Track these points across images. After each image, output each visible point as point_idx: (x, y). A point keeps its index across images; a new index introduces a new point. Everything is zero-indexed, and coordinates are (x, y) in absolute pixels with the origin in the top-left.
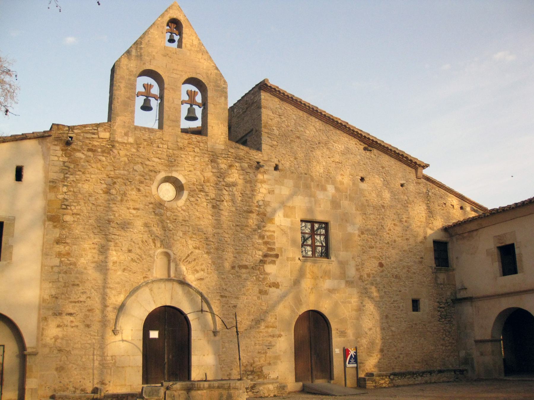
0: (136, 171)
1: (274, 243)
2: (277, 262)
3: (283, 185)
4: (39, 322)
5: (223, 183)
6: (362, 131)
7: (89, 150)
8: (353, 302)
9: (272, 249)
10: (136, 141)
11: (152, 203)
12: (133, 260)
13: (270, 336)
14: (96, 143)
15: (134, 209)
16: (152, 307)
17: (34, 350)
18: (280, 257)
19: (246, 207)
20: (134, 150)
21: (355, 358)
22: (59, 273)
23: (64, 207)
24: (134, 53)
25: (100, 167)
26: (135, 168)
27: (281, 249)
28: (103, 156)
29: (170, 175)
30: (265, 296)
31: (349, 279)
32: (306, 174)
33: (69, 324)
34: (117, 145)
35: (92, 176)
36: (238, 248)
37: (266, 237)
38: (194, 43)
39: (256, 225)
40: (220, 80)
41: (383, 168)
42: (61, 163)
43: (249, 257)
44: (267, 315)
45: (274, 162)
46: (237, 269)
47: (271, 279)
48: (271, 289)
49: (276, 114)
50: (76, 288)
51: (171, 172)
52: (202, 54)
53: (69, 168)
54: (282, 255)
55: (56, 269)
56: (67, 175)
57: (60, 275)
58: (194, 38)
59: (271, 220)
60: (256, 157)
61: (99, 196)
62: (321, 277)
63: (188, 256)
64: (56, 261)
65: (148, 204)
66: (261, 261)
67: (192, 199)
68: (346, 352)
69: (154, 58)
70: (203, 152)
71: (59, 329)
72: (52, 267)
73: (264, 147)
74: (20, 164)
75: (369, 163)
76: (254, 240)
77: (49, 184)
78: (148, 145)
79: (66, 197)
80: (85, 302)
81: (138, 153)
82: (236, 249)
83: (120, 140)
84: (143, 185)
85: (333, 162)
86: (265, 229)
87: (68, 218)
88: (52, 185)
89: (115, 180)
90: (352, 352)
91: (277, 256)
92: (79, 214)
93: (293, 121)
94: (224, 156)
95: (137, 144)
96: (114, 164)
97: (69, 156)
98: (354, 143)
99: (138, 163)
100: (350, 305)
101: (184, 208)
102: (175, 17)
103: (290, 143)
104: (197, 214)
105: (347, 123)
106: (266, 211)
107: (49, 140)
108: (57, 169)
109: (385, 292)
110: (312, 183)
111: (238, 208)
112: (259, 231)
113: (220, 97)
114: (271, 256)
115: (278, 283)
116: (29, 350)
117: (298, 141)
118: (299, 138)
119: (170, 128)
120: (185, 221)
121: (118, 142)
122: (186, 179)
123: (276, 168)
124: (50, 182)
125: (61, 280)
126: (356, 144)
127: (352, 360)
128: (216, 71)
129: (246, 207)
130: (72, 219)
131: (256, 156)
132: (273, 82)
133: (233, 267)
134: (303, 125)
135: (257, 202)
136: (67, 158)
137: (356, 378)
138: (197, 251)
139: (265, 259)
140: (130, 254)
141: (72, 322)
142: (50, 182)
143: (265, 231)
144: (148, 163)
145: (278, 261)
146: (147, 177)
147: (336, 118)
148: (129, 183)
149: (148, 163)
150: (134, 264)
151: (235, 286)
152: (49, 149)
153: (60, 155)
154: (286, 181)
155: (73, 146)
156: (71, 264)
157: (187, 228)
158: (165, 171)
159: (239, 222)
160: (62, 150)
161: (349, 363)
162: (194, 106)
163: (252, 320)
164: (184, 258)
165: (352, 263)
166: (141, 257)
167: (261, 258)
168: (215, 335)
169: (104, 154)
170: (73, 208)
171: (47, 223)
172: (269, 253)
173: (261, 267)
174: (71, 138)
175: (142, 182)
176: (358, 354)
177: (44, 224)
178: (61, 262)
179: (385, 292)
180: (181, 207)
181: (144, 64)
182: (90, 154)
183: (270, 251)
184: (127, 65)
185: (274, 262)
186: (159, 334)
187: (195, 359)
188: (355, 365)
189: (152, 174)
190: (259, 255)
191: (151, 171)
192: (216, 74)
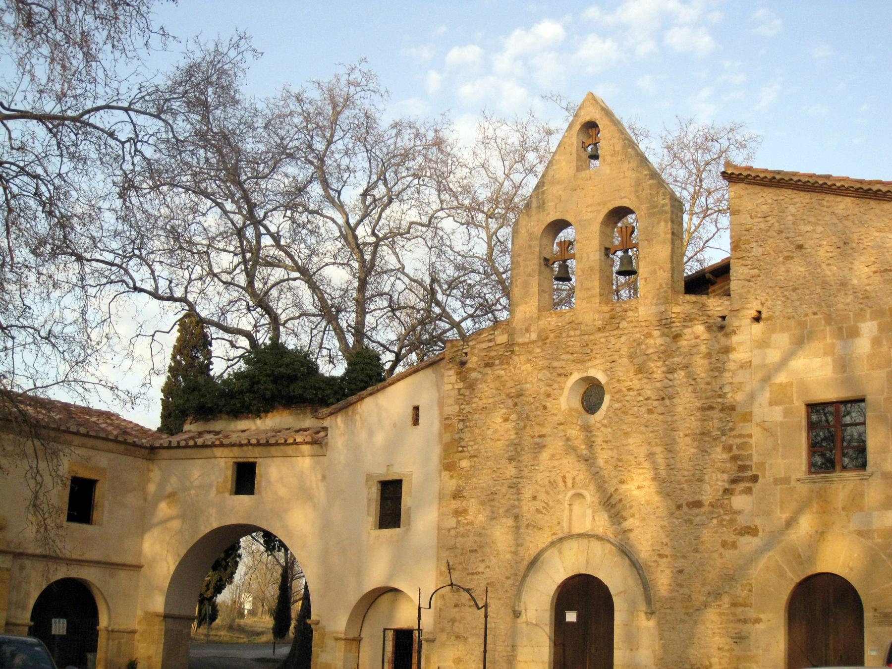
1: (750, 457)
2: (754, 490)
9: (742, 468)
10: (539, 336)
13: (740, 620)
14: (493, 354)
15: (540, 436)
17: (430, 636)
18: (760, 480)
19: (701, 402)
20: (538, 350)
23: (460, 449)
24: (534, 204)
28: (502, 369)
29: (585, 375)
30: (731, 551)
32: (815, 314)
37: (734, 447)
39: (718, 429)
42: (456, 391)
44: (734, 583)
45: (751, 308)
46: (685, 509)
47: (742, 521)
49: (756, 217)
50: (474, 554)
51: (586, 371)
52: (629, 162)
53: (465, 396)
54: (764, 477)
55: (453, 532)
56: (463, 406)
59: (747, 417)
61: (497, 426)
62: (843, 509)
64: (452, 522)
66: (726, 491)
67: (617, 405)
70: (632, 324)
71: (457, 609)
72: (449, 530)
74: (416, 404)
76: (713, 456)
78: (556, 337)
82: (684, 476)
83: (520, 341)
84: (550, 399)
86: (734, 433)
88: (446, 423)
89: (516, 400)
91: (755, 479)
92: (475, 456)
93: (790, 218)
96: (515, 378)
101: (605, 422)
102: (588, 119)
106: (735, 400)
107: (444, 362)
112: (724, 438)
115: (756, 527)
119: (585, 302)
121: (519, 345)
122: (608, 375)
123: (757, 319)
124: (445, 419)
129: (701, 402)
130: (469, 464)
133: (679, 507)
134: (812, 219)
135: (721, 388)
136: (461, 385)
139: (733, 486)
142: (445, 419)
145: (757, 487)
147: (870, 183)
148: (532, 400)
150: (540, 516)
151: (680, 538)
152: (442, 376)
153: (454, 381)
155: (469, 365)
156: (467, 524)
158: (579, 370)
163: (709, 593)
166: (548, 505)
167: (727, 485)
169: (504, 366)
170: (470, 448)
172: (740, 474)
173: (726, 502)
174: (466, 354)
175: (549, 396)
178: (458, 522)
180: (600, 422)
181: (549, 214)
183: (743, 472)
185: (748, 491)
186: (578, 617)
189: (562, 379)
190: (724, 481)
191: (560, 375)
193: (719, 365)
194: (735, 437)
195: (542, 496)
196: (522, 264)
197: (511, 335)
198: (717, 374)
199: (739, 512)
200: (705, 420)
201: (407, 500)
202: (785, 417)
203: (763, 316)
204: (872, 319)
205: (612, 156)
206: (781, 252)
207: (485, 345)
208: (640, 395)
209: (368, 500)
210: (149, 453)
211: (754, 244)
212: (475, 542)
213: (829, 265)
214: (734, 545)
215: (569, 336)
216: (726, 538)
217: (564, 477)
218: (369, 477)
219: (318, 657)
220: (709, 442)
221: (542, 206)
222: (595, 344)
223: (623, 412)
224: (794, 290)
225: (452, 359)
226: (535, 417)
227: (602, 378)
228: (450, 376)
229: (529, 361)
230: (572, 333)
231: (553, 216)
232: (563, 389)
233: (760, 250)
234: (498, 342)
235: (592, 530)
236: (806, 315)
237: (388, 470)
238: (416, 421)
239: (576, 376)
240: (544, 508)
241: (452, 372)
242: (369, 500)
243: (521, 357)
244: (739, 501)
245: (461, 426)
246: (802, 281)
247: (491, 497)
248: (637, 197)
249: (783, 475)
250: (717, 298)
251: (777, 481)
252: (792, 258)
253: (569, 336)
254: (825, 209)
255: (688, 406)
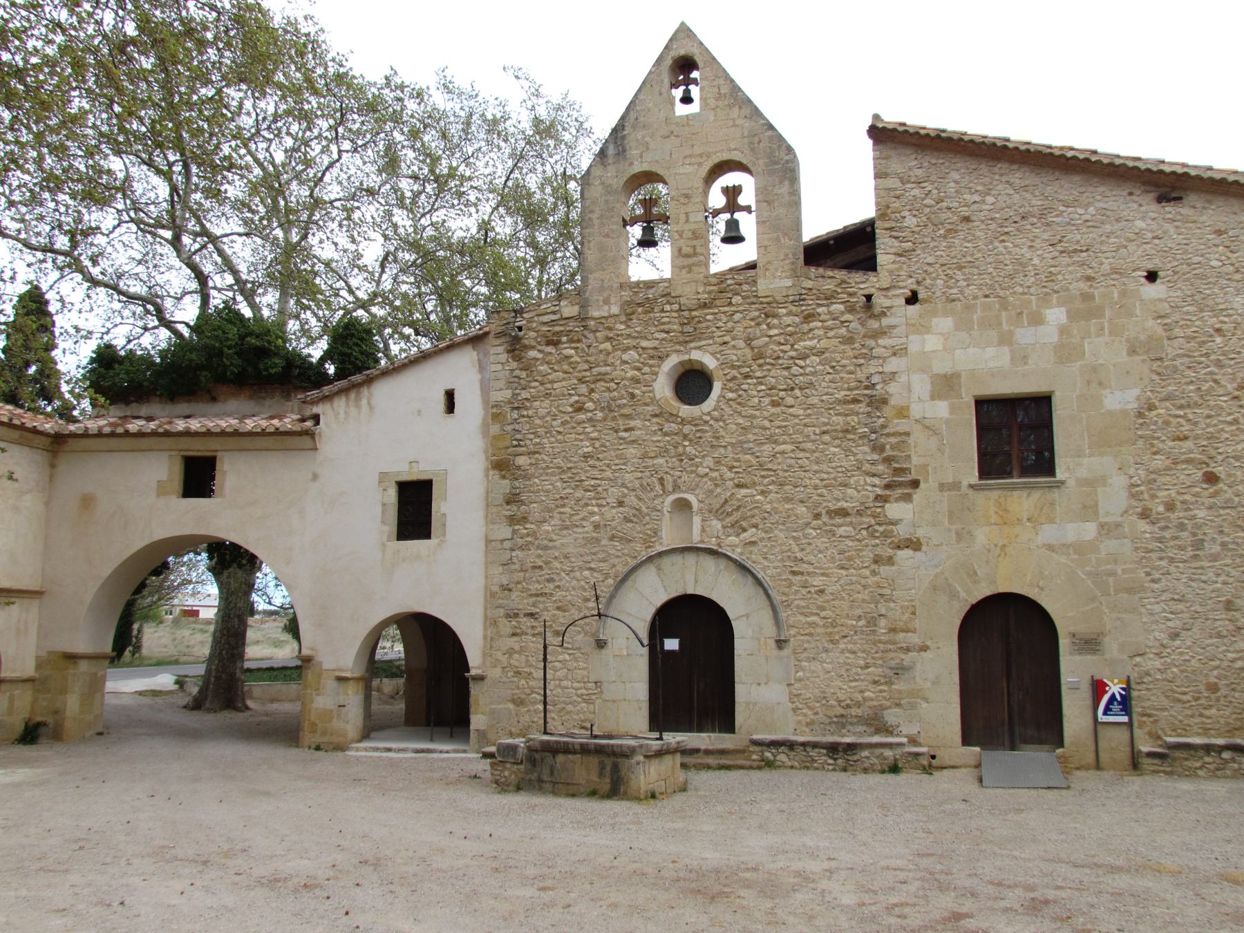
0: (626, 362)
1: (909, 456)
2: (915, 496)
3: (928, 333)
4: (485, 628)
5: (793, 354)
6: (1139, 159)
7: (549, 343)
8: (1119, 572)
9: (899, 471)
11: (656, 416)
12: (627, 520)
14: (558, 329)
15: (626, 430)
16: (662, 598)
17: (479, 672)
18: (922, 485)
21: (1125, 703)
22: (512, 550)
23: (515, 443)
24: (611, 151)
25: (566, 367)
26: (625, 357)
27: (925, 466)
29: (686, 357)
30: (887, 568)
31: (1106, 520)
32: (986, 296)
33: (529, 631)
34: (592, 323)
35: (556, 385)
36: (825, 476)
38: (722, 92)
40: (780, 146)
41: (1219, 233)
43: (849, 491)
46: (825, 518)
47: (902, 531)
48: (900, 553)
49: (909, 182)
51: (688, 353)
54: (926, 481)
55: (507, 544)
57: (514, 554)
58: (722, 81)
60: (862, 286)
63: (726, 501)
64: (506, 532)
65: (648, 417)
66: (877, 498)
67: (730, 395)
68: (1098, 688)
69: (648, 149)
71: (515, 639)
72: (502, 541)
73: (881, 259)
74: (449, 387)
75: (1172, 230)
77: (491, 411)
79: (517, 427)
80: (551, 595)
81: (628, 331)
82: (822, 480)
83: (596, 314)
85: (1062, 252)
86: (886, 431)
87: (522, 461)
88: (495, 414)
90: (1115, 689)
91: (915, 484)
93: (952, 184)
94: (791, 298)
95: (627, 315)
97: (518, 359)
98: (1125, 193)
99: (628, 349)
100: (1111, 580)
102: (682, 52)
103: (945, 237)
104: (741, 421)
105: (1095, 152)
108: (502, 384)
109: (1223, 544)
110: (1004, 313)
111: (824, 398)
113: (781, 182)
114: (901, 484)
115: (918, 540)
116: (473, 672)
117: (965, 226)
118: (967, 219)
120: (718, 438)
121: (595, 319)
122: (718, 359)
123: (912, 299)
125: (515, 560)
126: (1131, 194)
127: (1116, 707)
128: (770, 133)
131: (861, 283)
132: (891, 117)
134: (979, 188)
136: (515, 364)
137: (1128, 749)
138: (744, 491)
139: (888, 492)
140: (621, 509)
141: (533, 627)
143: (888, 435)
144: (644, 344)
145: (918, 496)
146: (646, 369)
147: (1062, 148)
149: (644, 344)
151: (820, 552)
152: (486, 354)
154: (935, 321)
157: (722, 450)
159: (828, 424)
160: (509, 352)
161: (1105, 713)
162: (737, 215)
164: (718, 506)
165: (1119, 482)
168: (780, 648)
170: (528, 442)
171: (491, 473)
174: (520, 329)
176: (1134, 694)
177: (487, 476)
178: (514, 532)
179: (1223, 544)
180: (709, 414)
181: (632, 164)
182: (550, 349)
184: (600, 177)
185: (907, 498)
186: (680, 644)
187: (742, 692)
188: (1125, 719)
191: (652, 357)
192: (771, 139)
193: (864, 351)
194: (888, 435)
195: (632, 500)
196: (596, 222)
197: (584, 306)
198: (862, 361)
199: (894, 523)
200: (847, 415)
201: (440, 507)
202: (951, 414)
203: (920, 296)
204: (1059, 305)
205: (717, 99)
206: (942, 224)
207: (546, 319)
208: (761, 384)
209: (380, 506)
210: (52, 443)
211: (907, 213)
212: (540, 556)
213: (1003, 241)
214: (890, 561)
215: (663, 311)
216: (879, 551)
217: (662, 479)
218: (383, 477)
219: (312, 702)
220: (853, 440)
221: (622, 153)
222: (699, 322)
223: (739, 404)
224: (960, 268)
225: (499, 335)
226: (619, 406)
227: (710, 362)
228: (497, 351)
229: (608, 339)
230: (667, 308)
231: (637, 168)
232: (656, 374)
233: (914, 220)
234: (565, 315)
235: (702, 542)
236: (975, 298)
237: (411, 468)
238: (450, 407)
239: (673, 360)
240: (634, 515)
241: (500, 349)
242: (384, 505)
243: (598, 334)
244: (894, 510)
245: (515, 415)
246: (969, 259)
247: (560, 502)
248: (752, 150)
249: (951, 480)
250: (861, 273)
251: (942, 487)
252: (956, 231)
253: (663, 311)
254: (997, 177)
255: (824, 398)
